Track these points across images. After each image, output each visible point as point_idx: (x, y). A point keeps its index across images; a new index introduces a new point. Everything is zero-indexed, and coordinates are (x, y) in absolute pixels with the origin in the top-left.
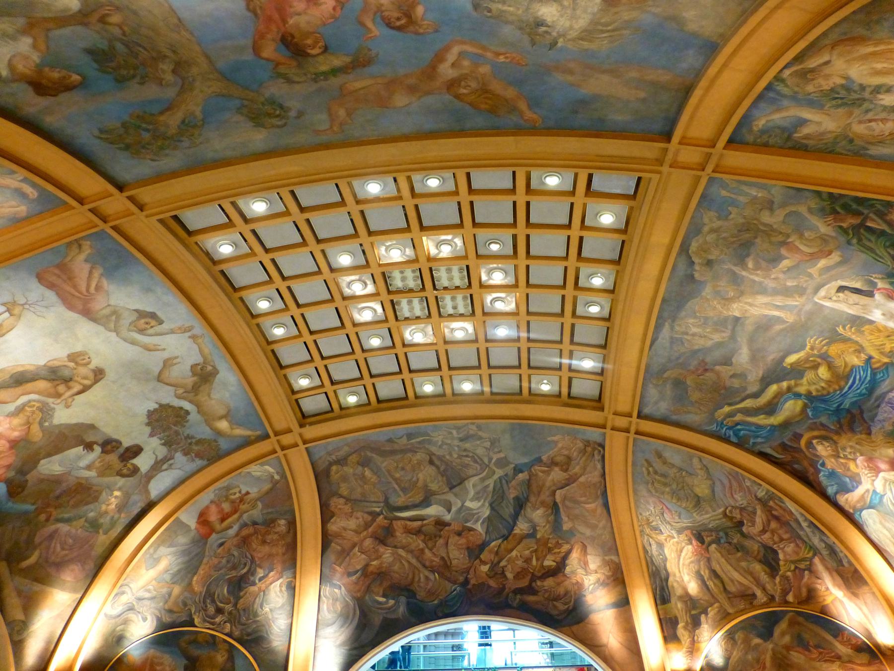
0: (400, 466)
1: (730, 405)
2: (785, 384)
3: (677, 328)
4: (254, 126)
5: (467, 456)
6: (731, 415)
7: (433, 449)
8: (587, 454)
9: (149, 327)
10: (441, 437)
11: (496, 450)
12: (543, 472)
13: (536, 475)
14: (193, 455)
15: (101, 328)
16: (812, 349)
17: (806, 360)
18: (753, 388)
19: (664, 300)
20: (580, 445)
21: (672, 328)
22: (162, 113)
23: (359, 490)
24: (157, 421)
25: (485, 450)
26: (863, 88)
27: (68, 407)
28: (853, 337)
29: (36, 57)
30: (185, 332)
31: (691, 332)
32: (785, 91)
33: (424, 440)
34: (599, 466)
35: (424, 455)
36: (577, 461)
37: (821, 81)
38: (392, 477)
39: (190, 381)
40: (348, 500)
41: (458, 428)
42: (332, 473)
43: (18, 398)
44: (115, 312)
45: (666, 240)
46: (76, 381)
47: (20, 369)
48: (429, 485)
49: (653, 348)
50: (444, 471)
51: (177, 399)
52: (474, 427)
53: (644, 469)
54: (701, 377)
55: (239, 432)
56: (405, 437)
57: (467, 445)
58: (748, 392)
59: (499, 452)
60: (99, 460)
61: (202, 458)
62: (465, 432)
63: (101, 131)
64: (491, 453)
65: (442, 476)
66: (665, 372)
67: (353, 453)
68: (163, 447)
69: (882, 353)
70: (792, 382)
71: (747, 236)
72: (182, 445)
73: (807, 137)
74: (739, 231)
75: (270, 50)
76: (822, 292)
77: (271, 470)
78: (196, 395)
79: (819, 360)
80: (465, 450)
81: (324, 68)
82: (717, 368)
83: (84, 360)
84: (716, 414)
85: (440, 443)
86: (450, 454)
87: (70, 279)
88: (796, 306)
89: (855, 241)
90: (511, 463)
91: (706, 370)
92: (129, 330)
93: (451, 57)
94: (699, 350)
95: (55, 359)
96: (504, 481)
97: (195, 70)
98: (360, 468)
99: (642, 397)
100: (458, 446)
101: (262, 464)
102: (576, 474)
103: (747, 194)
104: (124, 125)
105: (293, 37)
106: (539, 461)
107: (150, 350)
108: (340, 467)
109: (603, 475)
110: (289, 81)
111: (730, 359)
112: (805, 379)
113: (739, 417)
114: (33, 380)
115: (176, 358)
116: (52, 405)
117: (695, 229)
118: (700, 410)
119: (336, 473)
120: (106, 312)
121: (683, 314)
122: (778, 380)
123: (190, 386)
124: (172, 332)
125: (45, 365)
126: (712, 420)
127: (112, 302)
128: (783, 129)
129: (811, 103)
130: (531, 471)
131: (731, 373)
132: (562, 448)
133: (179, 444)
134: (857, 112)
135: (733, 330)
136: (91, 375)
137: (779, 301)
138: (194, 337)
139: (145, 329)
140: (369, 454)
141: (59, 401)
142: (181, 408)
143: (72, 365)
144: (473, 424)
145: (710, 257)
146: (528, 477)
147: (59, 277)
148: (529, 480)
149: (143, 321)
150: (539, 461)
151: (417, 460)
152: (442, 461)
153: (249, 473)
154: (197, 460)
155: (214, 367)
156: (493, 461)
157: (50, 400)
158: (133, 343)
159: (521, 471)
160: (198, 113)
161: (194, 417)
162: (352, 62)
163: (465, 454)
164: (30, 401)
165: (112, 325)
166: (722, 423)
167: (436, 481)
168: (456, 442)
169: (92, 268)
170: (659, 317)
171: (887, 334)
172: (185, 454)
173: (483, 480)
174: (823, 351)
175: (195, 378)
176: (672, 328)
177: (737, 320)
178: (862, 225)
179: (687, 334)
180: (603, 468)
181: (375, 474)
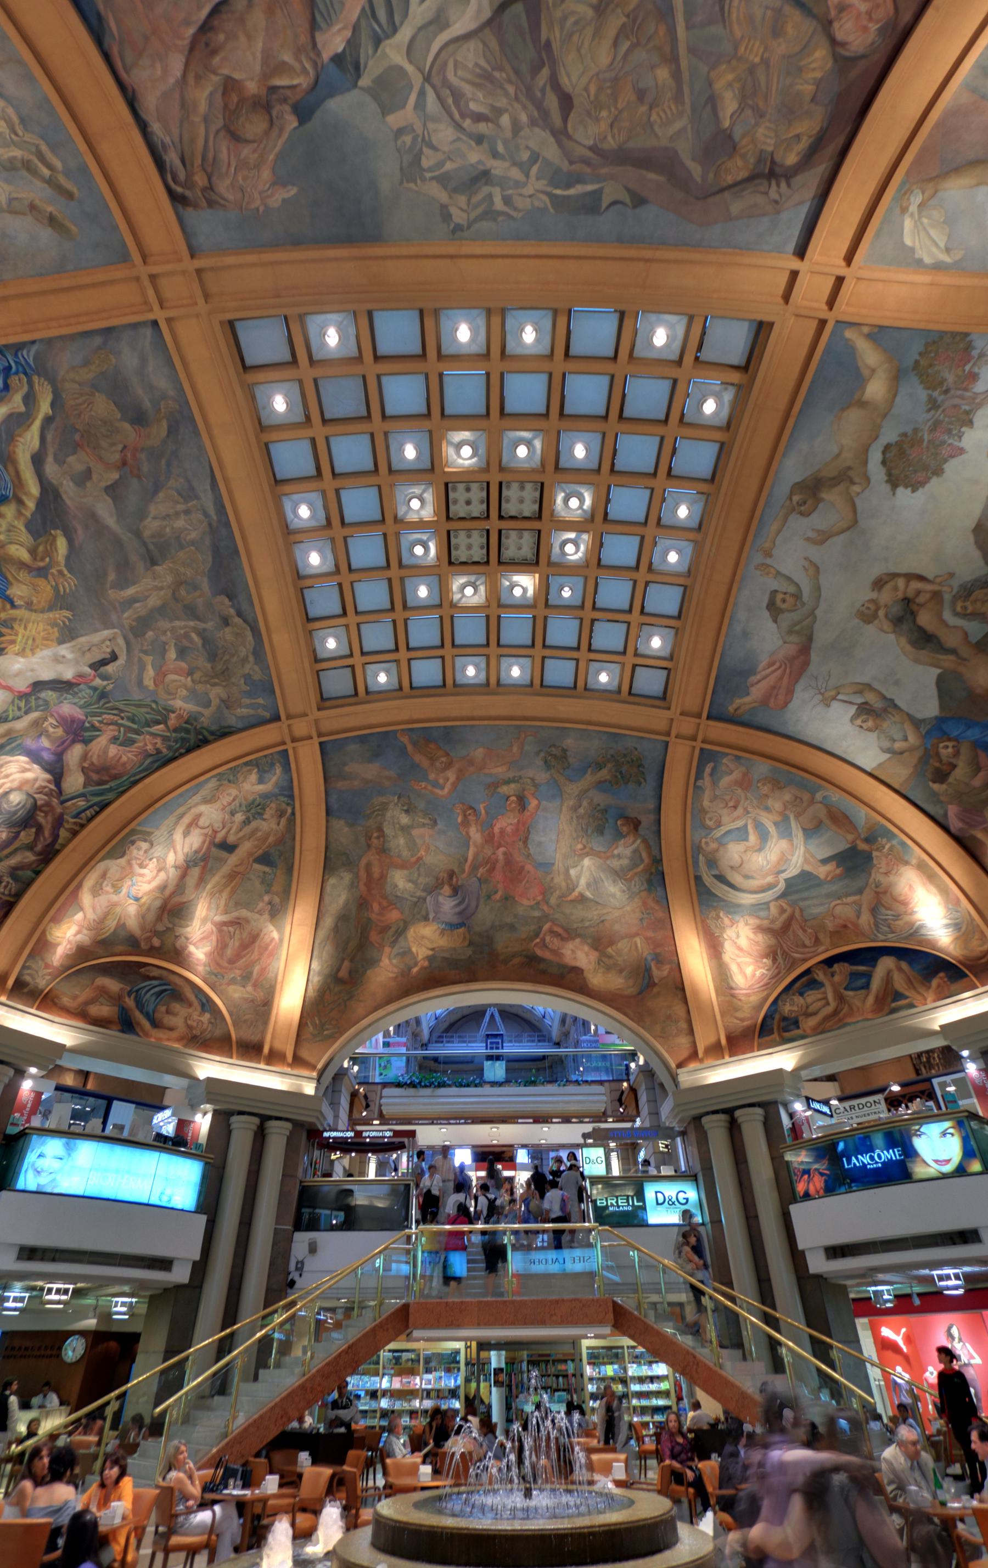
0: (643, 109)
1: (48, 420)
2: (31, 505)
3: (200, 516)
5: (479, 118)
6: (30, 399)
7: (551, 152)
8: (198, 161)
9: (787, 597)
10: (529, 190)
11: (408, 139)
12: (282, 68)
13: (297, 58)
14: (967, 368)
15: (817, 626)
16: (60, 572)
17: (48, 553)
18: (51, 468)
19: (236, 552)
20: (223, 187)
21: (206, 514)
23: (781, 48)
24: (926, 468)
25: (435, 142)
26: (254, 818)
27: (952, 575)
28: (51, 615)
30: (768, 566)
31: (182, 516)
32: (282, 798)
33: (568, 186)
34: (156, 127)
35: (579, 135)
36: (213, 129)
37: (273, 812)
38: (677, 75)
39: (831, 496)
40: (827, 25)
41: (490, 214)
42: (804, 144)
43: (955, 627)
44: (790, 632)
45: (276, 638)
46: (905, 592)
47: (908, 648)
48: (590, 13)
49: (209, 471)
50: (543, 64)
51: (872, 481)
52: (459, 217)
53: (58, 164)
54: (120, 447)
56: (604, 205)
57: (475, 156)
58: (50, 459)
59: (400, 132)
61: (969, 347)
62: (475, 200)
63: (640, 784)
64: (418, 128)
65: (548, 44)
66: (169, 432)
67: (729, 187)
68: (975, 420)
69: (14, 619)
70: (28, 514)
71: (220, 667)
72: (957, 401)
73: (250, 771)
74: (227, 669)
75: (534, 803)
76: (121, 641)
77: (908, 223)
78: (849, 468)
79: (42, 564)
80: (479, 139)
81: (513, 786)
82: (115, 476)
84: (48, 388)
85: (534, 170)
86: (516, 128)
87: (773, 688)
88: (123, 612)
89: (154, 706)
90: (367, 90)
91: (124, 463)
92: (803, 604)
93: (448, 786)
94: (155, 492)
95: (882, 630)
96: (382, 14)
97: (571, 803)
98: (737, 135)
99: (170, 363)
100: (495, 155)
101: (912, 250)
102: (198, 78)
103: (247, 706)
106: (304, 112)
107: (817, 568)
108: (778, 158)
109: (132, 102)
110: (533, 780)
111: (115, 499)
112: (23, 529)
113: (16, 402)
114: (921, 629)
115: (808, 539)
116: (955, 591)
117: (258, 653)
118: (73, 381)
119: (798, 137)
120: (794, 638)
121: (207, 542)
122: (41, 503)
123: (841, 488)
124: (778, 573)
125: (894, 632)
126: (42, 369)
127: (781, 642)
128: (265, 772)
129: (265, 796)
130: (315, 64)
131: (95, 477)
132: (258, 167)
133: (955, 406)
134: (244, 802)
135: (145, 544)
136: (888, 587)
137: (140, 609)
138: (768, 554)
139: (793, 595)
140: (696, 170)
141: (945, 589)
142: (884, 463)
143: (881, 613)
144: (458, 228)
145: (228, 630)
146: (319, 37)
148: (314, 26)
149: (784, 606)
150: (304, 112)
151: (598, 120)
152: (539, 105)
153: (948, 250)
154: (975, 353)
155: (792, 493)
156: (413, 98)
157: (947, 597)
158: (817, 589)
159: (338, 59)
160: (589, 771)
161: (889, 435)
163: (483, 127)
164: (956, 614)
166: (25, 373)
167: (572, 20)
168: (498, 168)
170: (228, 524)
171: (38, 641)
172: (974, 377)
173: (439, 21)
174: (50, 577)
175: (824, 495)
176: (206, 514)
177: (154, 562)
178: (164, 721)
179: (187, 512)
180: (143, 126)
181: (713, 101)
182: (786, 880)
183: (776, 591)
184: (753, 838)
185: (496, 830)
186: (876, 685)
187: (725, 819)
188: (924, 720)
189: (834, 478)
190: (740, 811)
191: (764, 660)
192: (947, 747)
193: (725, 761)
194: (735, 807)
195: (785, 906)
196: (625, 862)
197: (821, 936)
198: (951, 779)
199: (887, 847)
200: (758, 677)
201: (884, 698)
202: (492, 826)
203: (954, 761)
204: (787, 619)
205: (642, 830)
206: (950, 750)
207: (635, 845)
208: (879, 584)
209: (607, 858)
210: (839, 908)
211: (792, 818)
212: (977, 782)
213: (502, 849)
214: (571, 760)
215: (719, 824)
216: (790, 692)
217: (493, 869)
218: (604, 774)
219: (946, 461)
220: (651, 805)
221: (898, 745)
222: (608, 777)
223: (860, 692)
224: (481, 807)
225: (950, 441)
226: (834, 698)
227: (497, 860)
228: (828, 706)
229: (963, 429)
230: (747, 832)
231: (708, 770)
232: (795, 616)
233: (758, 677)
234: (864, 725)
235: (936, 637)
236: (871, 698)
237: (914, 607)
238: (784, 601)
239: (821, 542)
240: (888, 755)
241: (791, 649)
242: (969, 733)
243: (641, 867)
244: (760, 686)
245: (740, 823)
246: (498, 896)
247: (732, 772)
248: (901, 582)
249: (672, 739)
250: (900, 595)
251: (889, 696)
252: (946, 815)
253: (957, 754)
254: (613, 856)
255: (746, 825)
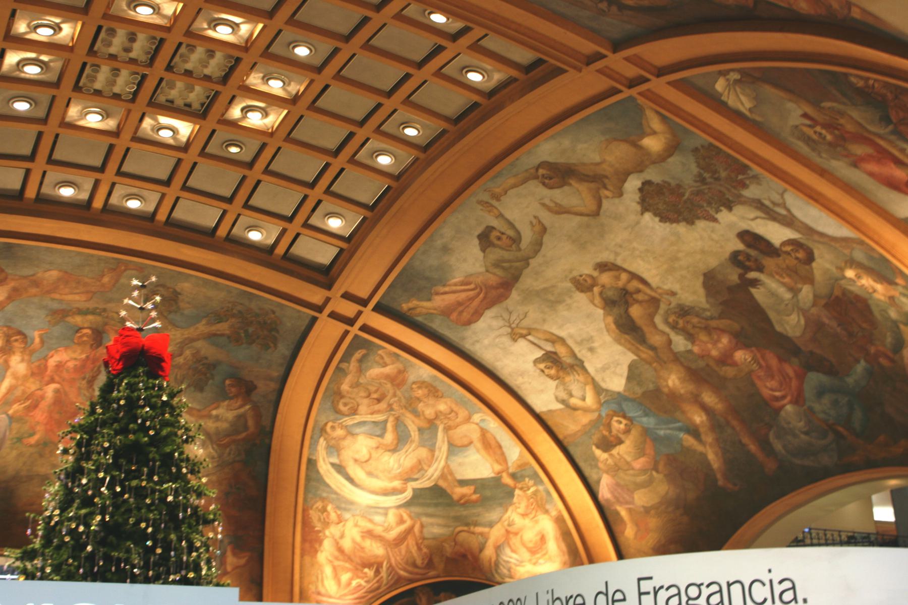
4: (180, 294)
9: (504, 237)
15: (526, 272)
22: (222, 335)
27: (673, 294)
29: (226, 403)
30: (492, 206)
44: (497, 264)
47: (613, 326)
55: (656, 124)
60: (777, 277)
68: (734, 208)
81: (91, 317)
83: (586, 281)
87: (459, 304)
104: (251, 343)
105: (92, 345)
114: (629, 317)
115: (544, 205)
116: (672, 305)
120: (499, 272)
125: (604, 308)
127: (483, 269)
139: (510, 238)
143: (596, 290)
147: (462, 312)
157: (663, 307)
160: (204, 322)
162: (67, 316)
164: (666, 322)
165: (522, 263)
169: (437, 294)
182: (414, 490)
183: (493, 228)
184: (389, 437)
185: (52, 362)
186: (570, 342)
187: (363, 409)
188: (607, 391)
189: (588, 176)
190: (383, 405)
191: (458, 277)
192: (620, 422)
193: (380, 352)
194: (379, 400)
195: (405, 517)
196: (224, 426)
197: (436, 560)
198: (615, 451)
199: (532, 489)
200: (447, 289)
201: (574, 355)
202: (46, 359)
203: (622, 437)
204: (495, 254)
205: (255, 397)
206: (622, 426)
207: (242, 410)
208: (603, 267)
209: (202, 417)
210: (463, 534)
211: (441, 428)
212: (638, 464)
213: (53, 386)
214: (182, 305)
215: (354, 412)
216: (477, 315)
217: (34, 406)
218: (224, 327)
219: (699, 218)
220: (276, 373)
221: (574, 401)
222: (227, 332)
223: (553, 342)
224: (36, 335)
225: (708, 209)
226: (523, 336)
227: (42, 397)
228: (515, 340)
229: (722, 208)
230: (384, 429)
231: (358, 355)
232: (506, 255)
233: (447, 289)
234: (547, 371)
235: (642, 330)
236: (561, 350)
237: (630, 300)
238: (499, 239)
239: (558, 213)
240: (560, 406)
241: (493, 280)
242: (645, 420)
243: (244, 435)
244: (446, 297)
245: (379, 418)
246: (33, 440)
247: (385, 365)
248: (624, 277)
249: (323, 317)
250: (621, 284)
251: (579, 355)
252: (598, 482)
253: (627, 431)
254: (209, 416)
255: (386, 421)
